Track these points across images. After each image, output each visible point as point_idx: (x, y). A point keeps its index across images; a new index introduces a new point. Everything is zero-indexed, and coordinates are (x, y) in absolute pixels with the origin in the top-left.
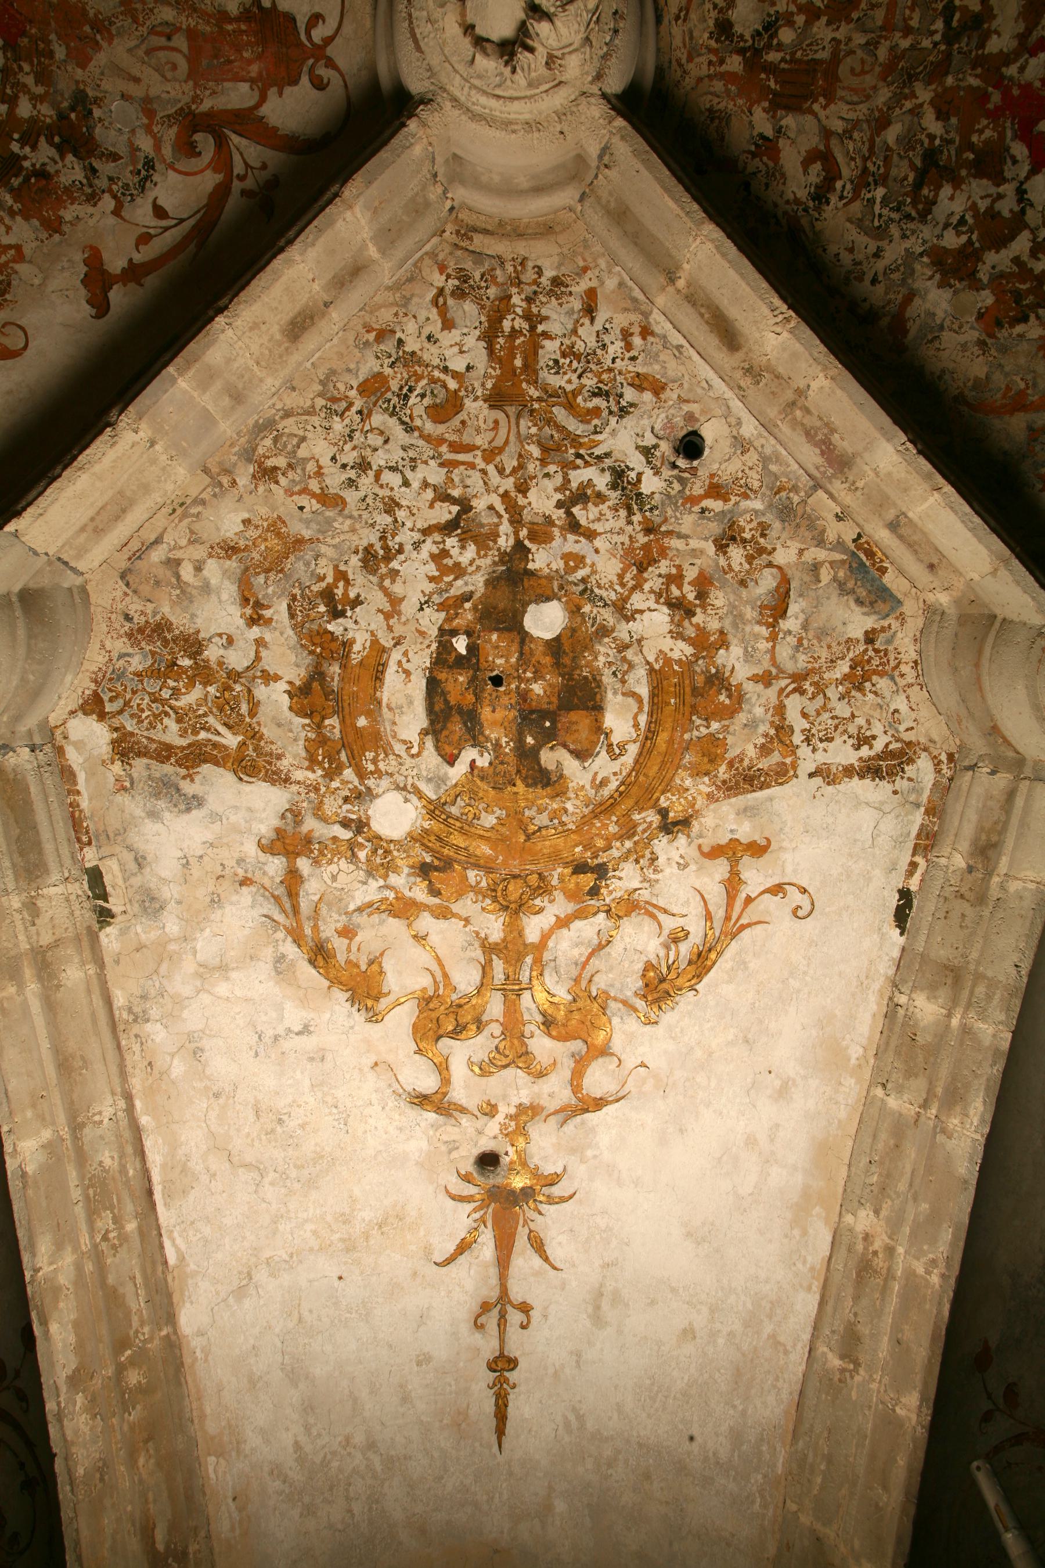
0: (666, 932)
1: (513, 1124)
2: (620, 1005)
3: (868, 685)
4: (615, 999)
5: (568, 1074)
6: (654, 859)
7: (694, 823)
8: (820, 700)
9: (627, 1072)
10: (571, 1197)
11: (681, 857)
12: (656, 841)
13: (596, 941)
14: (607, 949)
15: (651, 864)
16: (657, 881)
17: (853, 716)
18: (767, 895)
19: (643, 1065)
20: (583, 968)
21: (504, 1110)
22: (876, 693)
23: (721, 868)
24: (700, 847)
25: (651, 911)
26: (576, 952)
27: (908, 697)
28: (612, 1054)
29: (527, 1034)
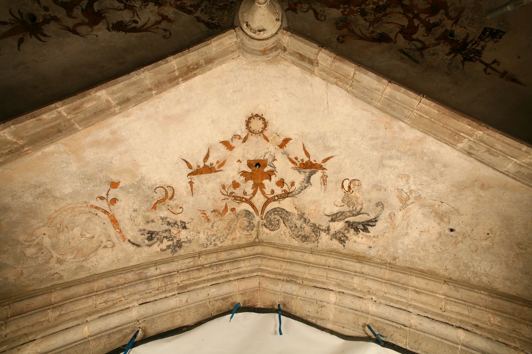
0: (134, 19)
1: (49, 17)
2: (106, 22)
3: (223, 10)
4: (106, 20)
5: (76, 22)
6: (147, 5)
7: (163, 7)
8: (211, 6)
9: (91, 34)
10: (44, 42)
11: (153, 10)
12: (151, 3)
13: (116, 8)
14: (117, 11)
15: (145, 6)
16: (143, 9)
17: (215, 14)
18: (162, 30)
19: (97, 36)
20: (107, 9)
21: (50, 13)
22: (223, 13)
23: (159, 18)
24: (159, 11)
25: (135, 13)
26: (108, 5)
27: (228, 18)
28: (92, 28)
29: (77, 7)
